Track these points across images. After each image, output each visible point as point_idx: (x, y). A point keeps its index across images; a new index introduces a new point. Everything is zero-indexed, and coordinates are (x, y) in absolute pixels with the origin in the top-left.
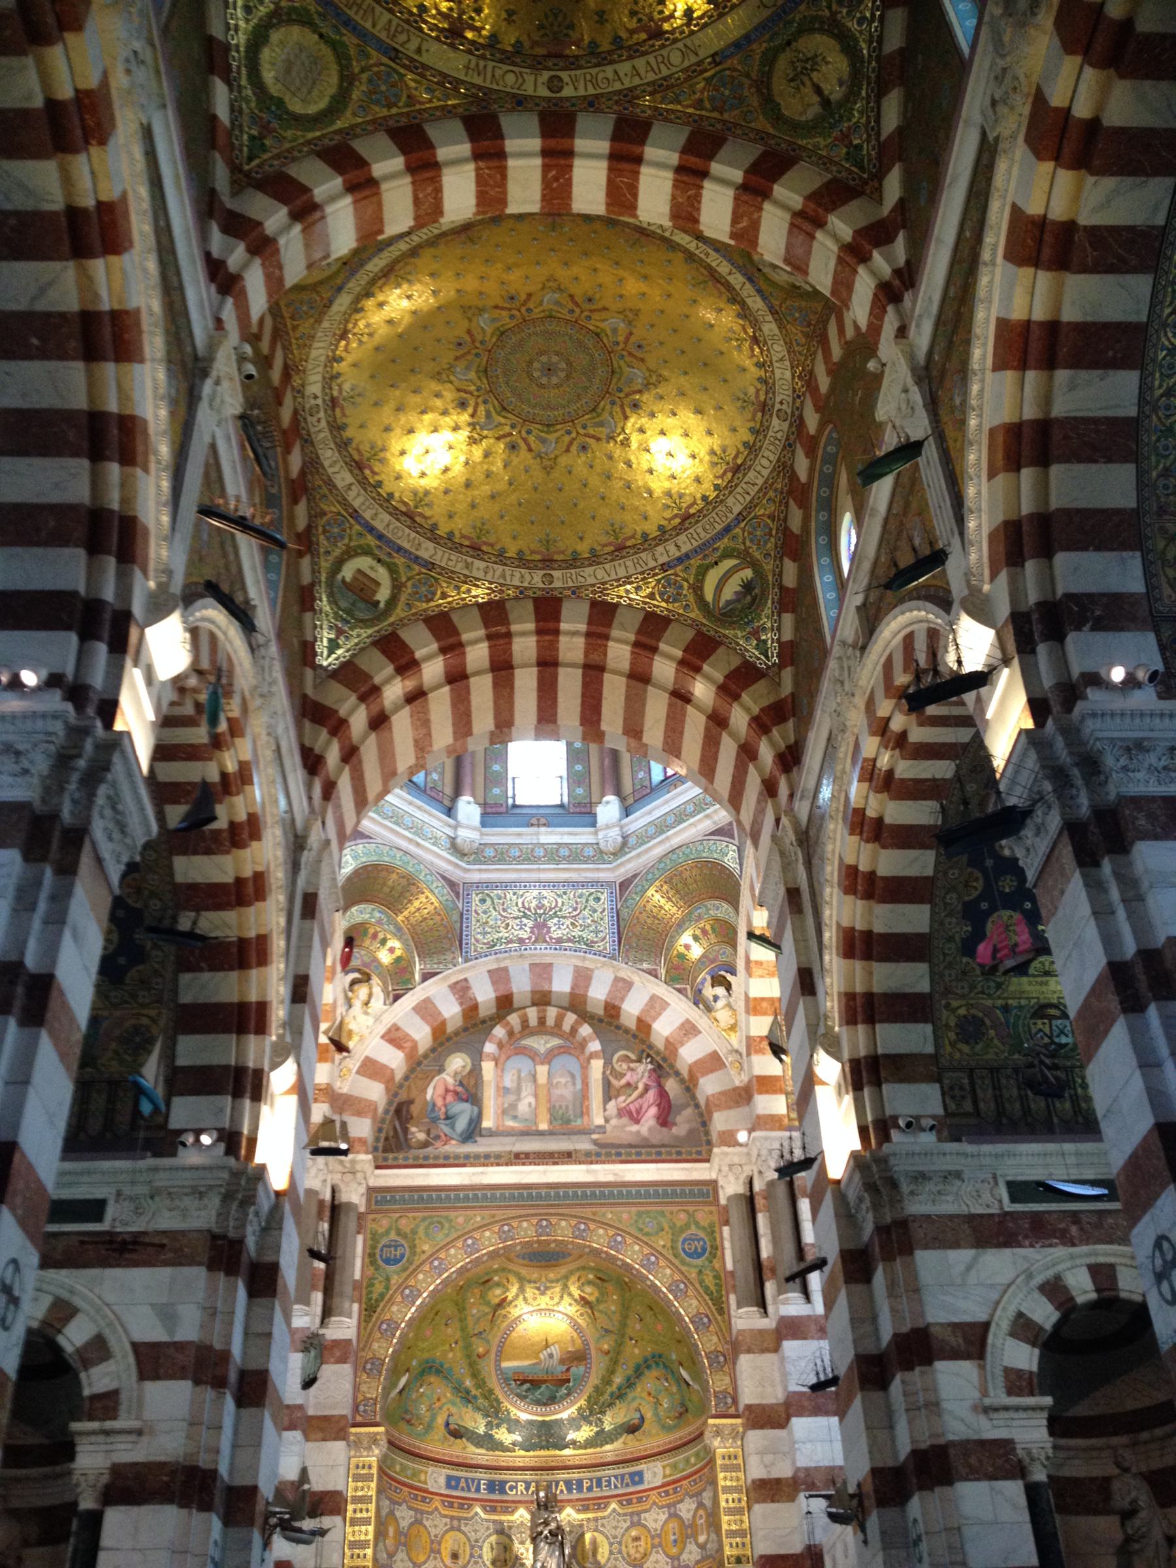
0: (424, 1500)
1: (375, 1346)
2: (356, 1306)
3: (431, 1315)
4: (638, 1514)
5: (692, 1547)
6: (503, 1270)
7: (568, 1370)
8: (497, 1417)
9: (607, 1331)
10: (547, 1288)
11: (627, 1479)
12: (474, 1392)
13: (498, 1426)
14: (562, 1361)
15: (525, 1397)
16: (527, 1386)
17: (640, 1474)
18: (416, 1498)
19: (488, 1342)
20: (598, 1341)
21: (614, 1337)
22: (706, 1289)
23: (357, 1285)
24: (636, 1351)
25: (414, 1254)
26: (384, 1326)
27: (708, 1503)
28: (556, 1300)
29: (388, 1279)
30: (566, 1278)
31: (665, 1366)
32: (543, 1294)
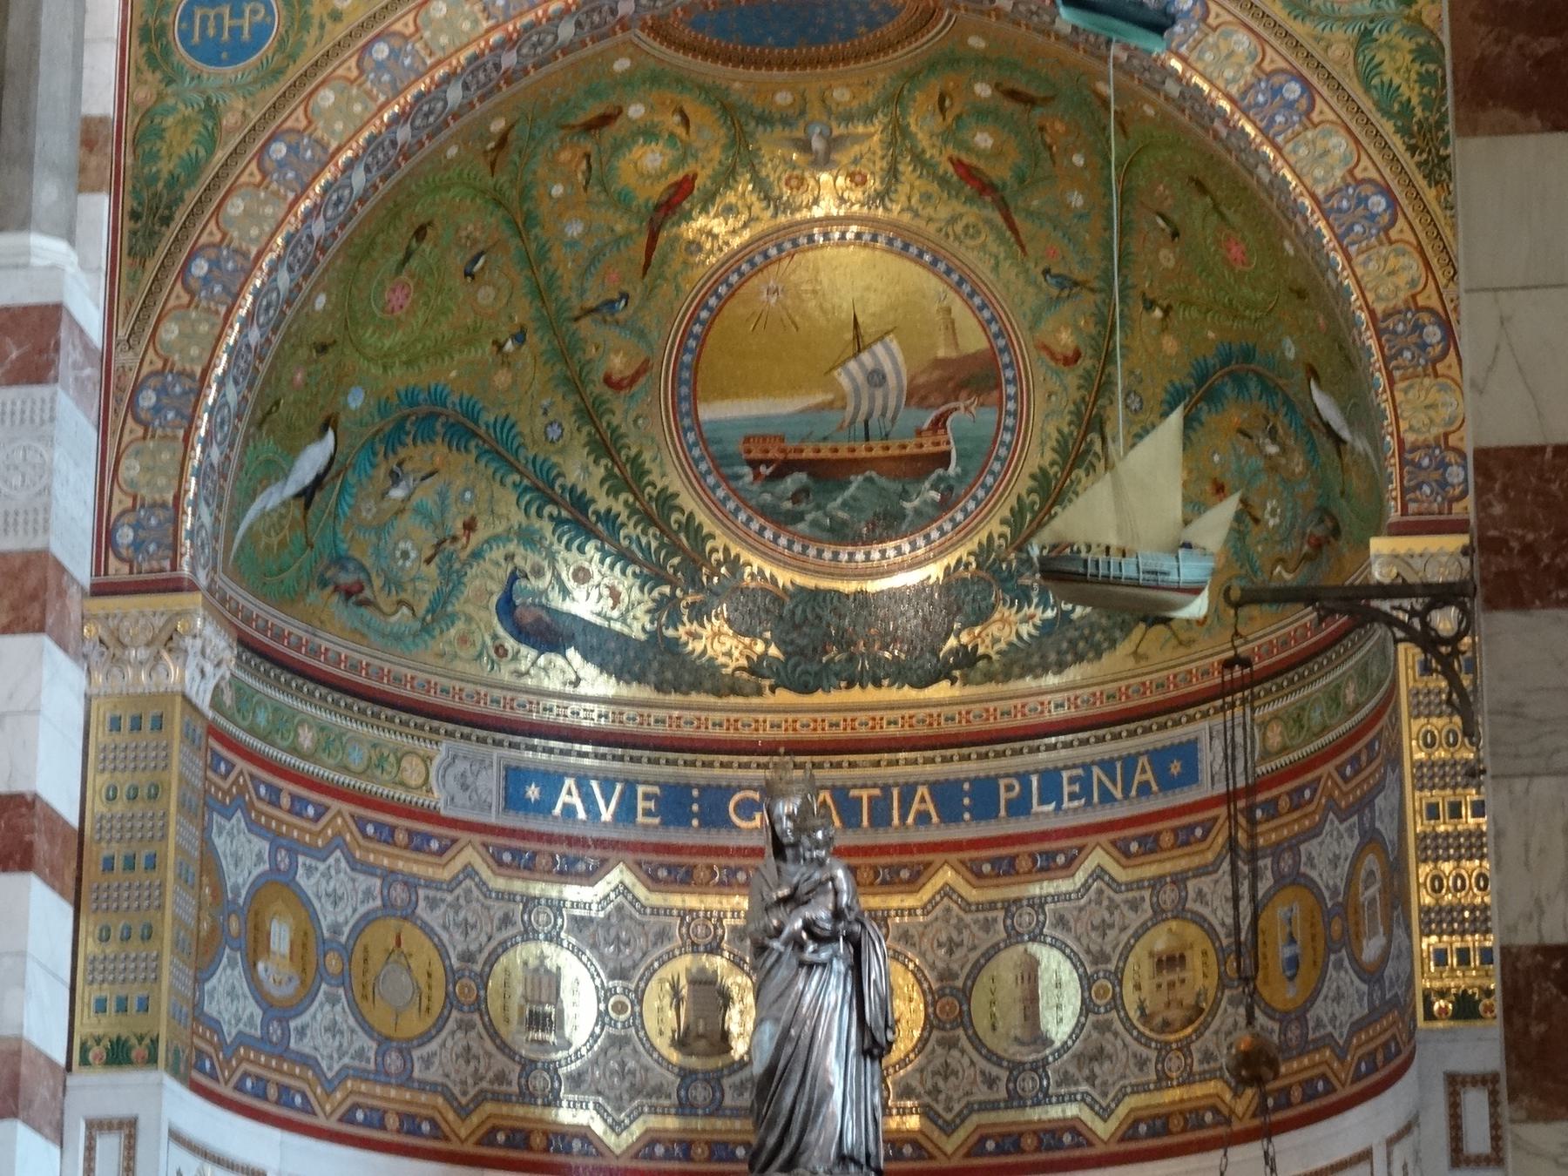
0: (417, 844)
1: (171, 332)
2: (98, 209)
3: (401, 234)
4: (1179, 879)
5: (1344, 979)
6: (655, 79)
7: (939, 423)
8: (694, 582)
9: (1068, 284)
10: (833, 143)
11: (1144, 774)
12: (603, 502)
13: (700, 613)
14: (916, 396)
15: (798, 517)
16: (793, 482)
17: (1187, 752)
18: (386, 835)
19: (642, 334)
20: (1036, 319)
21: (1088, 301)
22: (1387, 98)
23: (89, 135)
24: (1170, 344)
25: (305, 22)
26: (200, 267)
27: (1386, 829)
28: (873, 184)
29: (211, 110)
30: (896, 99)
31: (1269, 389)
32: (824, 162)
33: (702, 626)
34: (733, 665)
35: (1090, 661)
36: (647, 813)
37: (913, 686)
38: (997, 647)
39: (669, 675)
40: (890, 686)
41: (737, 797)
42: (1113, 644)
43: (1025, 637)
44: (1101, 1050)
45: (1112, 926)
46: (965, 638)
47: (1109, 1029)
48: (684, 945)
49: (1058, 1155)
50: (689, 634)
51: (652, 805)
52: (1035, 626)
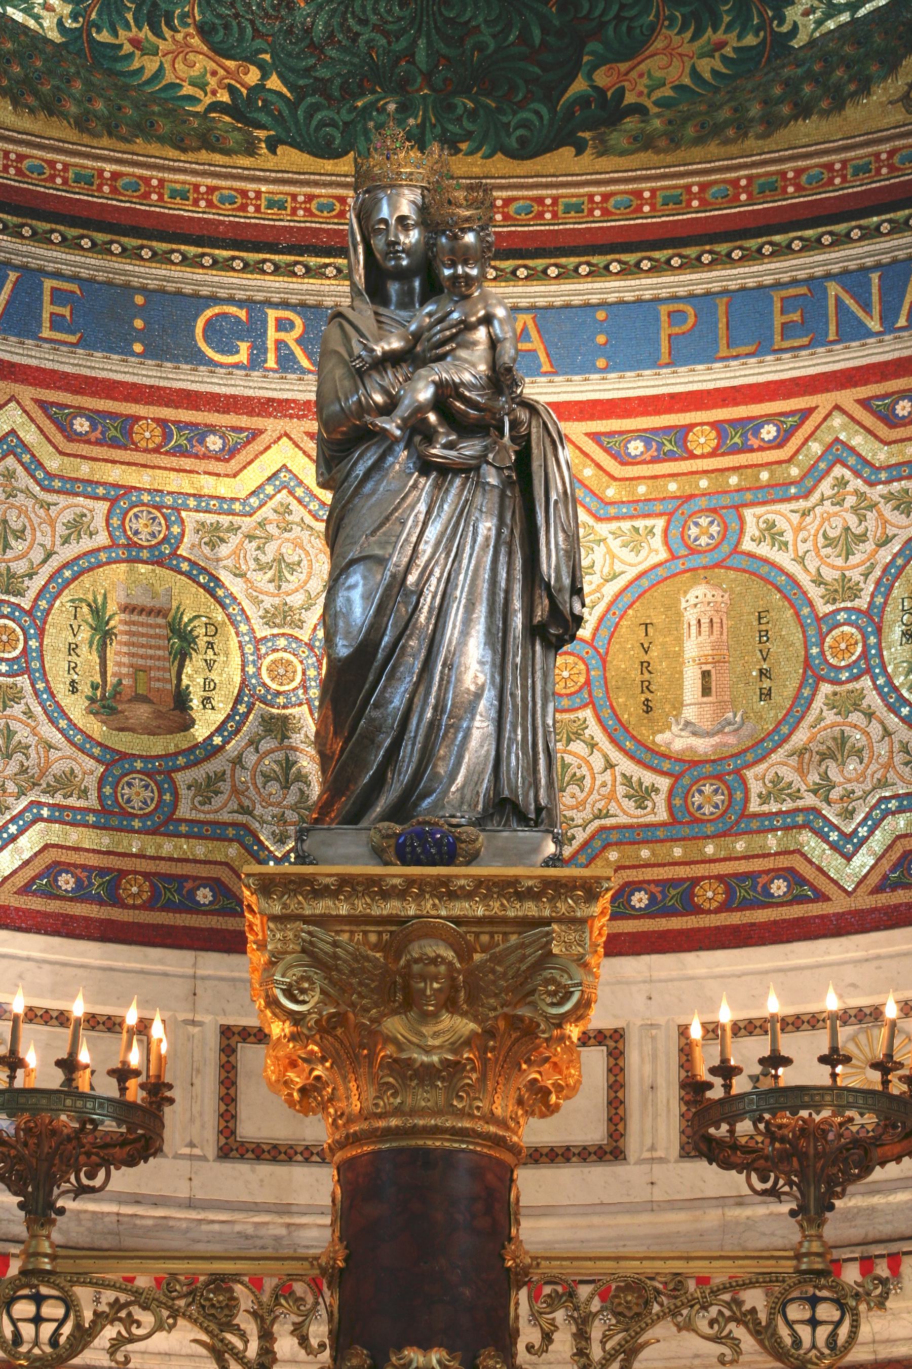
33: (159, 35)
34: (208, 100)
35: (825, 114)
36: (57, 323)
37: (512, 155)
38: (658, 94)
39: (100, 106)
40: (471, 153)
41: (209, 313)
42: (865, 88)
43: (707, 76)
44: (842, 740)
45: (862, 538)
46: (602, 78)
47: (856, 707)
48: (114, 545)
49: (761, 916)
50: (135, 42)
51: (66, 311)
52: (724, 59)
